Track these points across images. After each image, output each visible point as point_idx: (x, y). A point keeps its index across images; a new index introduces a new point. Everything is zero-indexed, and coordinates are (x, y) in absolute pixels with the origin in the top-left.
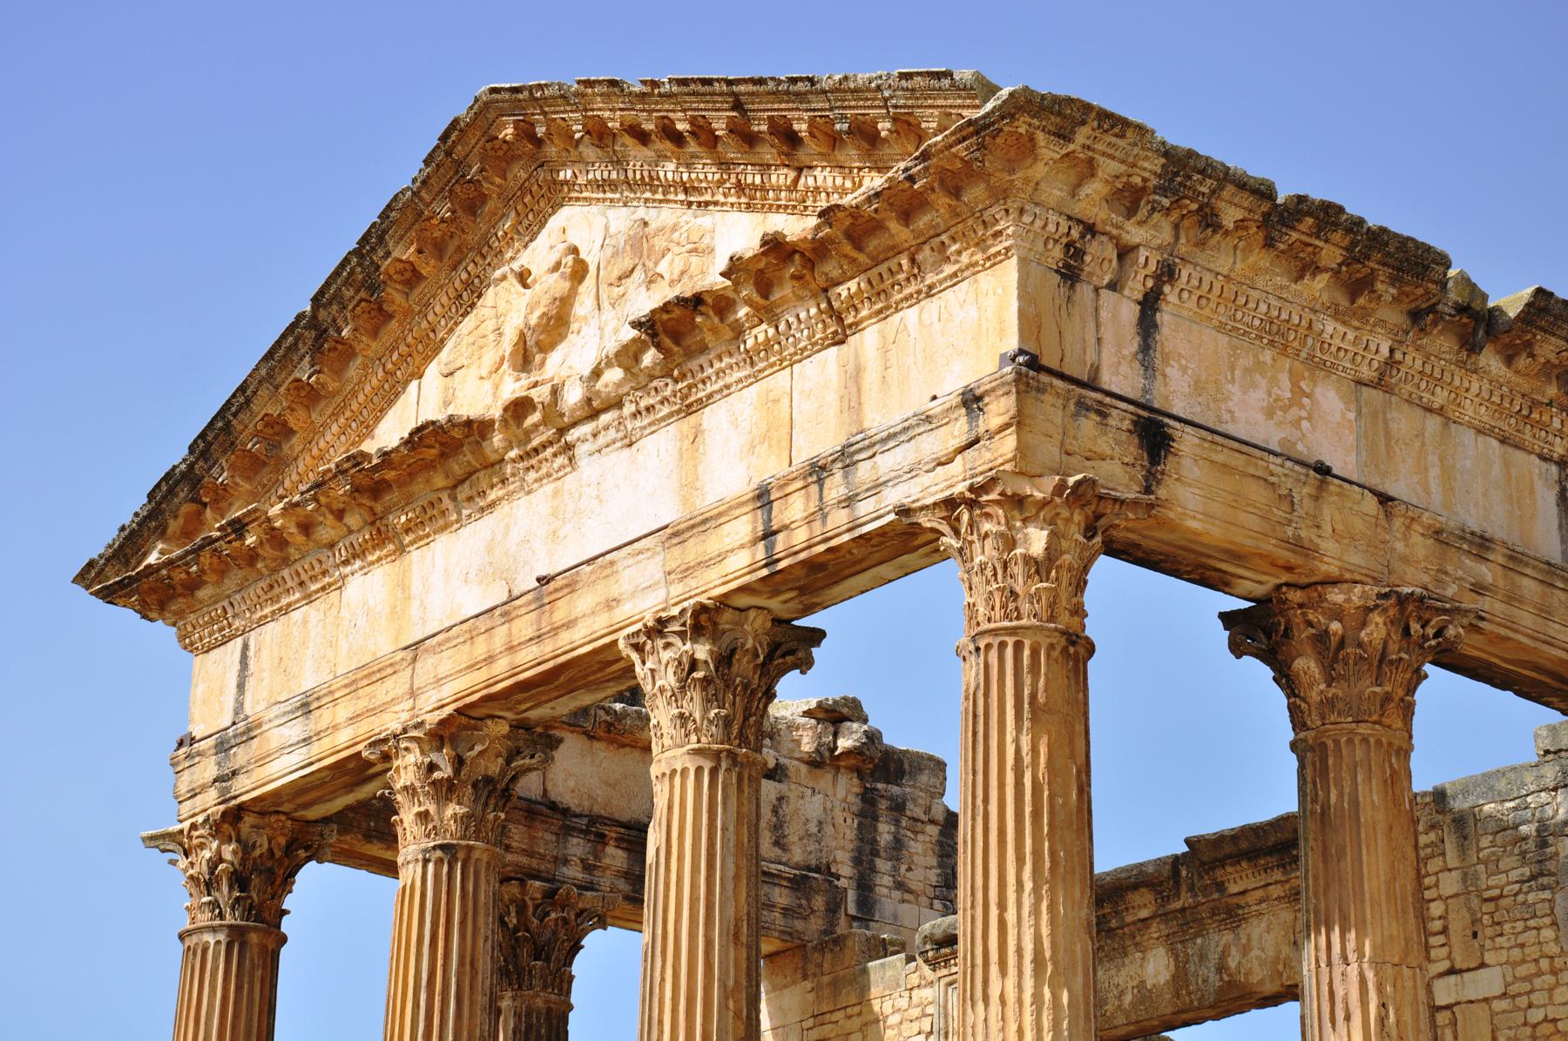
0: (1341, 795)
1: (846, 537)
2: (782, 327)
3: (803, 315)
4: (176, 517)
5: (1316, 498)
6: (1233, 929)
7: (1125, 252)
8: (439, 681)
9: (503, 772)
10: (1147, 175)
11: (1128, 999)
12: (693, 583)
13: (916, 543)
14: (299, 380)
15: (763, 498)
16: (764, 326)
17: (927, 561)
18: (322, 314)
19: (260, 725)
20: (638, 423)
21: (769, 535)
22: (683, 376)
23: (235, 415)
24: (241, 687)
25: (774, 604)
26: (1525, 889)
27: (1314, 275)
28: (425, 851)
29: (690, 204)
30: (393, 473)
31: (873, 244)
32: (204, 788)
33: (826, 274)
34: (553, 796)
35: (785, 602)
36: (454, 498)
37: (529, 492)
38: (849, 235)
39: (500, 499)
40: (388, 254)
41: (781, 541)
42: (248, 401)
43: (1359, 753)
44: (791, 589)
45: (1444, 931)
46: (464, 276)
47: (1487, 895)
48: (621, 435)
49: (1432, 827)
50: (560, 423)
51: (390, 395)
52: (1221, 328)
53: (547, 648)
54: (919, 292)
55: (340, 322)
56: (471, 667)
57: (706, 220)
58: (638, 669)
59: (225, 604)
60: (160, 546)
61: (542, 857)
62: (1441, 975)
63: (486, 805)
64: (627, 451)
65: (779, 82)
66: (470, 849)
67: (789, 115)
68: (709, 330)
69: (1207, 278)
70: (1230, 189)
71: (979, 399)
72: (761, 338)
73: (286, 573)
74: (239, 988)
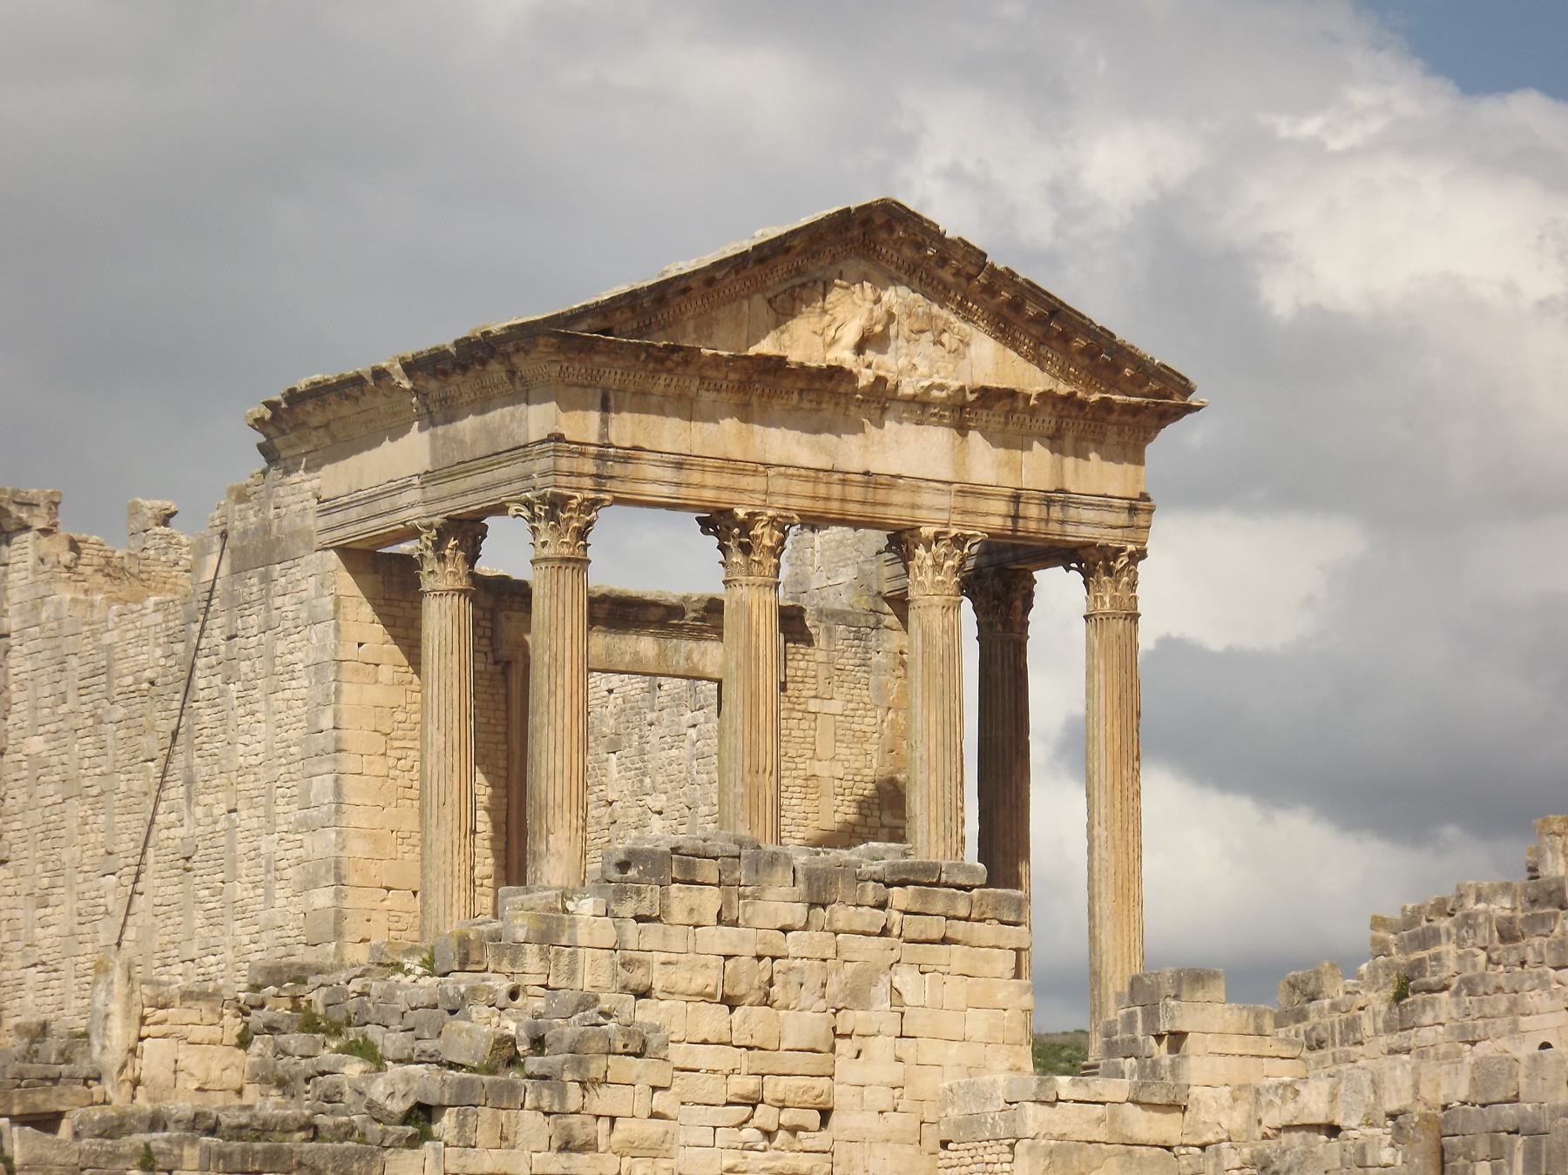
1: (1057, 537)
2: (1034, 421)
3: (1047, 420)
8: (788, 495)
11: (627, 658)
12: (967, 519)
15: (1016, 498)
19: (639, 459)
21: (1015, 517)
22: (969, 413)
26: (857, 669)
29: (955, 313)
32: (580, 475)
41: (1021, 523)
47: (838, 667)
50: (890, 395)
51: (734, 298)
53: (868, 510)
57: (967, 328)
59: (607, 371)
60: (590, 321)
64: (914, 427)
65: (1092, 322)
71: (1136, 509)
72: (1022, 419)
73: (664, 376)
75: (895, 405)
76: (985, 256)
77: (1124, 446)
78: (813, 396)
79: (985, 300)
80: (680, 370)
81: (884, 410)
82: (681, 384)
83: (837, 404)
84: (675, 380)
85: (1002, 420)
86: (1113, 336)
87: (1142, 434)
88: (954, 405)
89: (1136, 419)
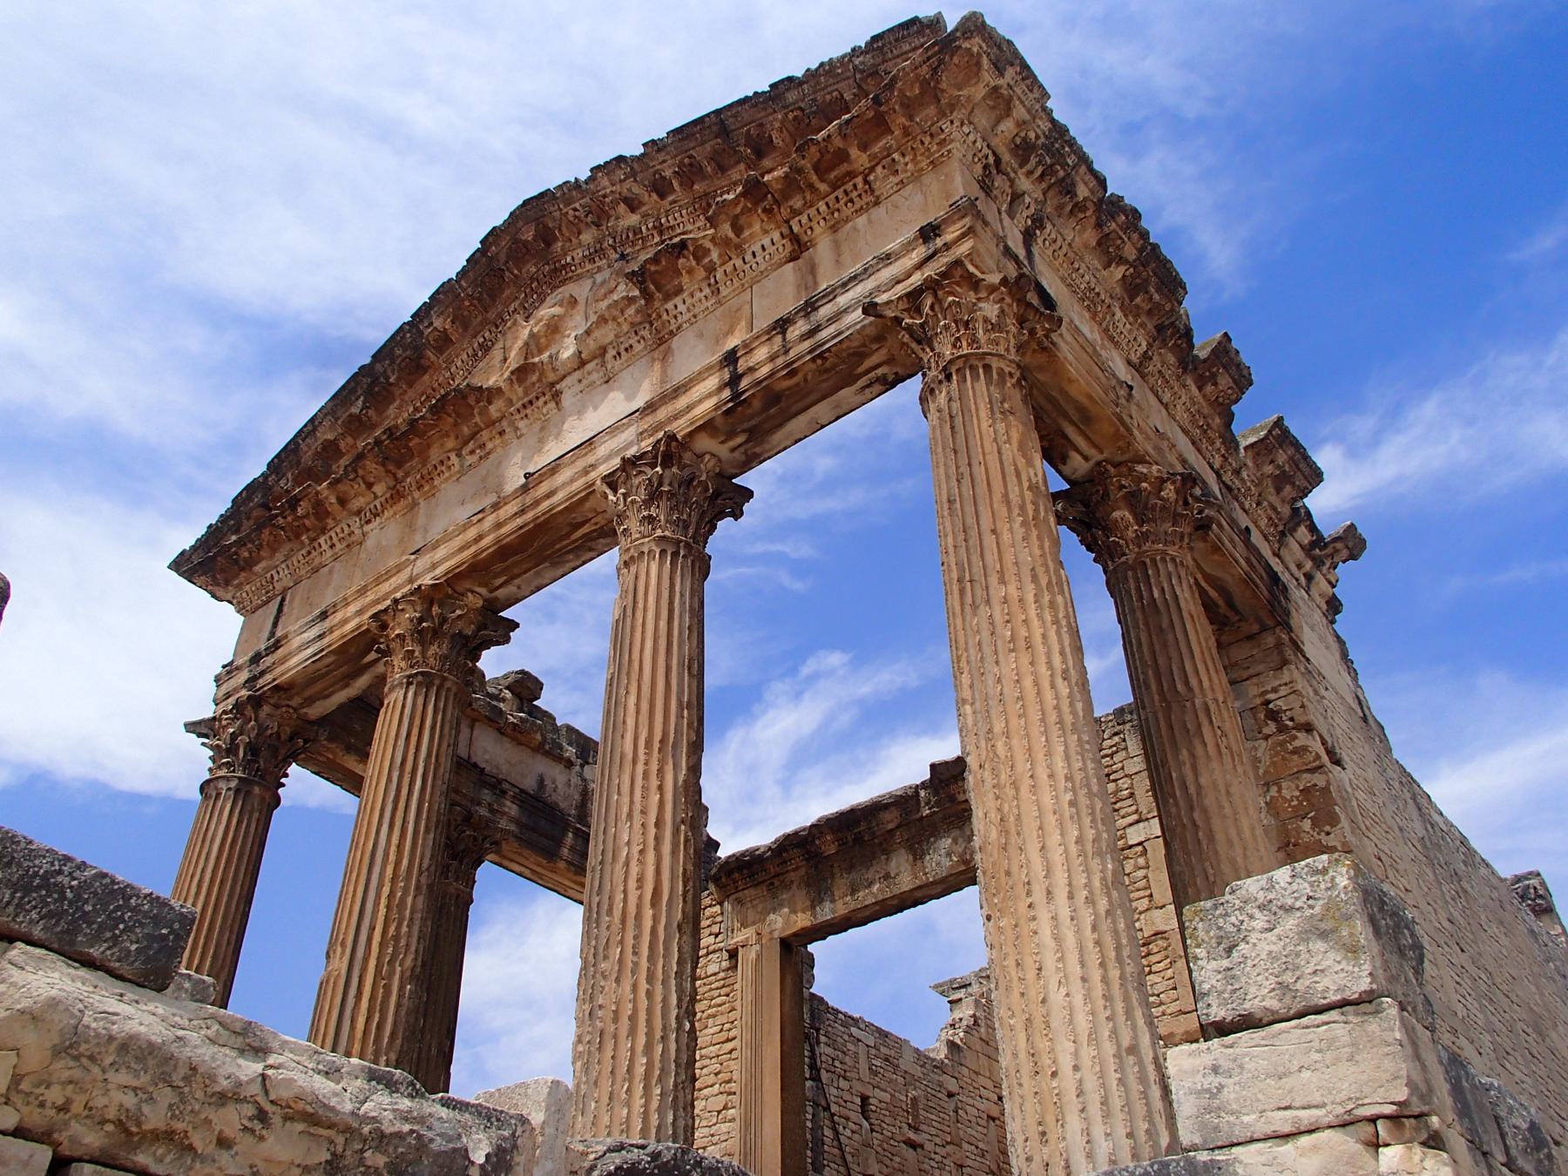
0: (1163, 590)
2: (748, 257)
3: (766, 242)
4: (248, 519)
5: (1128, 401)
6: (960, 828)
7: (1016, 197)
8: (434, 566)
9: (475, 636)
10: (1039, 132)
13: (860, 370)
14: (351, 415)
15: (731, 358)
16: (732, 262)
17: (860, 398)
18: (378, 367)
20: (618, 362)
21: (735, 379)
23: (303, 440)
24: (275, 624)
25: (723, 451)
27: (1118, 264)
28: (409, 677)
30: (417, 440)
31: (832, 175)
32: (236, 690)
33: (791, 207)
34: (474, 759)
35: (733, 450)
36: (459, 455)
37: (521, 436)
38: (816, 168)
39: (495, 447)
40: (431, 324)
41: (744, 383)
42: (314, 430)
43: (1171, 567)
44: (744, 431)
45: (1132, 795)
46: (481, 340)
48: (601, 374)
49: (1116, 734)
50: (552, 377)
52: (1063, 280)
53: (530, 515)
54: (867, 204)
55: (389, 373)
56: (462, 549)
58: (611, 497)
59: (274, 572)
61: (465, 796)
62: (1131, 825)
63: (459, 654)
64: (605, 386)
66: (444, 679)
67: (764, 121)
68: (690, 272)
69: (1060, 239)
70: (1083, 169)
73: (322, 540)
74: (239, 822)
75: (564, 384)
76: (620, 159)
77: (917, 177)
78: (471, 445)
79: (674, 202)
80: (330, 522)
81: (557, 396)
82: (341, 535)
83: (502, 433)
84: (333, 535)
85: (707, 291)
86: (790, 79)
87: (927, 140)
88: (633, 324)
89: (896, 133)
